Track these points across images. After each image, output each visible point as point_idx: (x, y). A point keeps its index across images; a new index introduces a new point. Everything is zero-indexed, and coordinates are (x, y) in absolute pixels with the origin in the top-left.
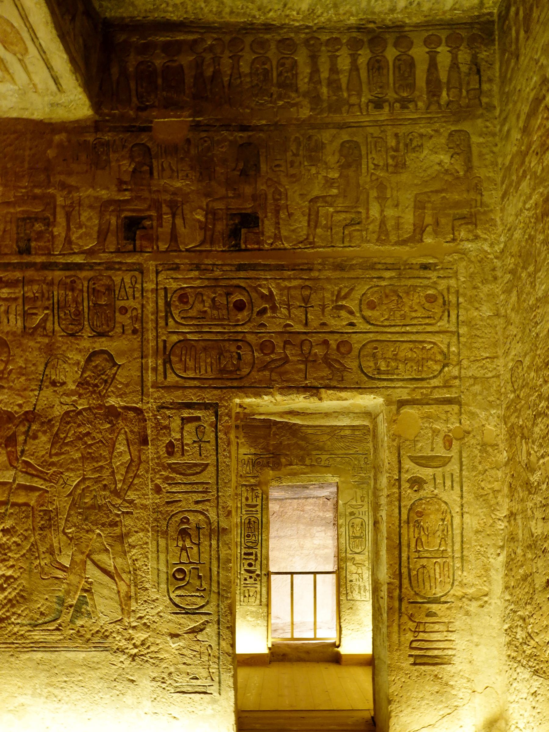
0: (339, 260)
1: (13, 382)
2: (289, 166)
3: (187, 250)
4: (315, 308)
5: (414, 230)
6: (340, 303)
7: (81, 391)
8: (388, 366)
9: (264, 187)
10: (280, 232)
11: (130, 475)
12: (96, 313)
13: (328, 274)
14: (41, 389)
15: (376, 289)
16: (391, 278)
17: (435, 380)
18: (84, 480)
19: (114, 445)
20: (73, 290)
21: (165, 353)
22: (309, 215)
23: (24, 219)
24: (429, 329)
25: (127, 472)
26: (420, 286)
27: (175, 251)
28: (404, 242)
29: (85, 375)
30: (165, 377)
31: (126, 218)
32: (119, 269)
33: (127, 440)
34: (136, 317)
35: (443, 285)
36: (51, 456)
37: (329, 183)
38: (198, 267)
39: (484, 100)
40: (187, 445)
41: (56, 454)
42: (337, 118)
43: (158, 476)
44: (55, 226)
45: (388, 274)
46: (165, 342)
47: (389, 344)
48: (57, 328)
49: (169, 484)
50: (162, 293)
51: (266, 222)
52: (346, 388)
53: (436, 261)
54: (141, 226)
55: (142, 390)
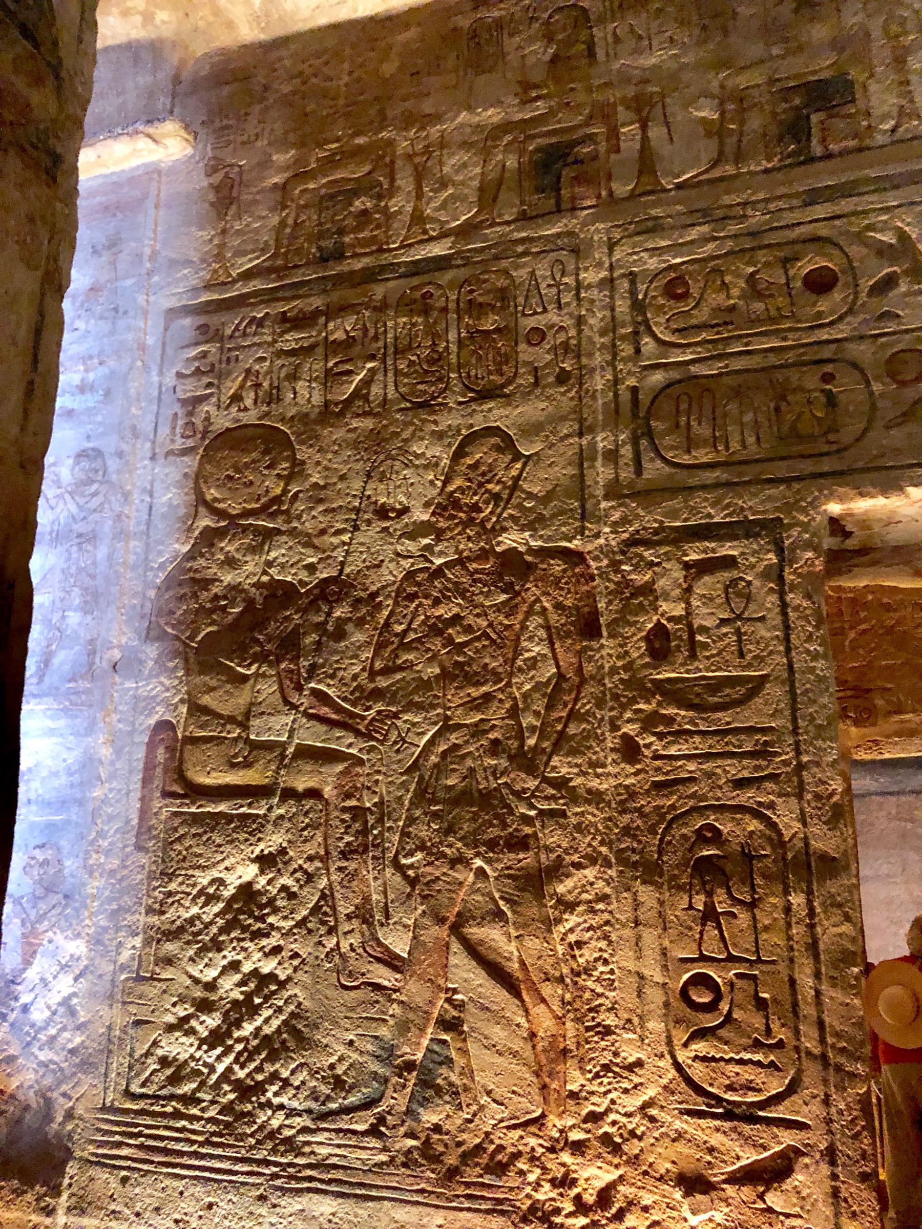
1: (299, 517)
3: (679, 187)
7: (442, 524)
10: (912, 101)
11: (555, 715)
12: (475, 352)
14: (356, 528)
18: (447, 728)
19: (518, 640)
20: (426, 311)
21: (635, 416)
23: (332, 197)
25: (549, 707)
29: (450, 488)
30: (639, 471)
31: (537, 150)
32: (525, 253)
33: (548, 628)
34: (566, 345)
36: (373, 674)
38: (705, 215)
40: (704, 630)
41: (386, 671)
43: (628, 715)
44: (391, 198)
46: (634, 390)
48: (391, 393)
49: (661, 736)
51: (873, 87)
54: (570, 159)
55: (583, 507)
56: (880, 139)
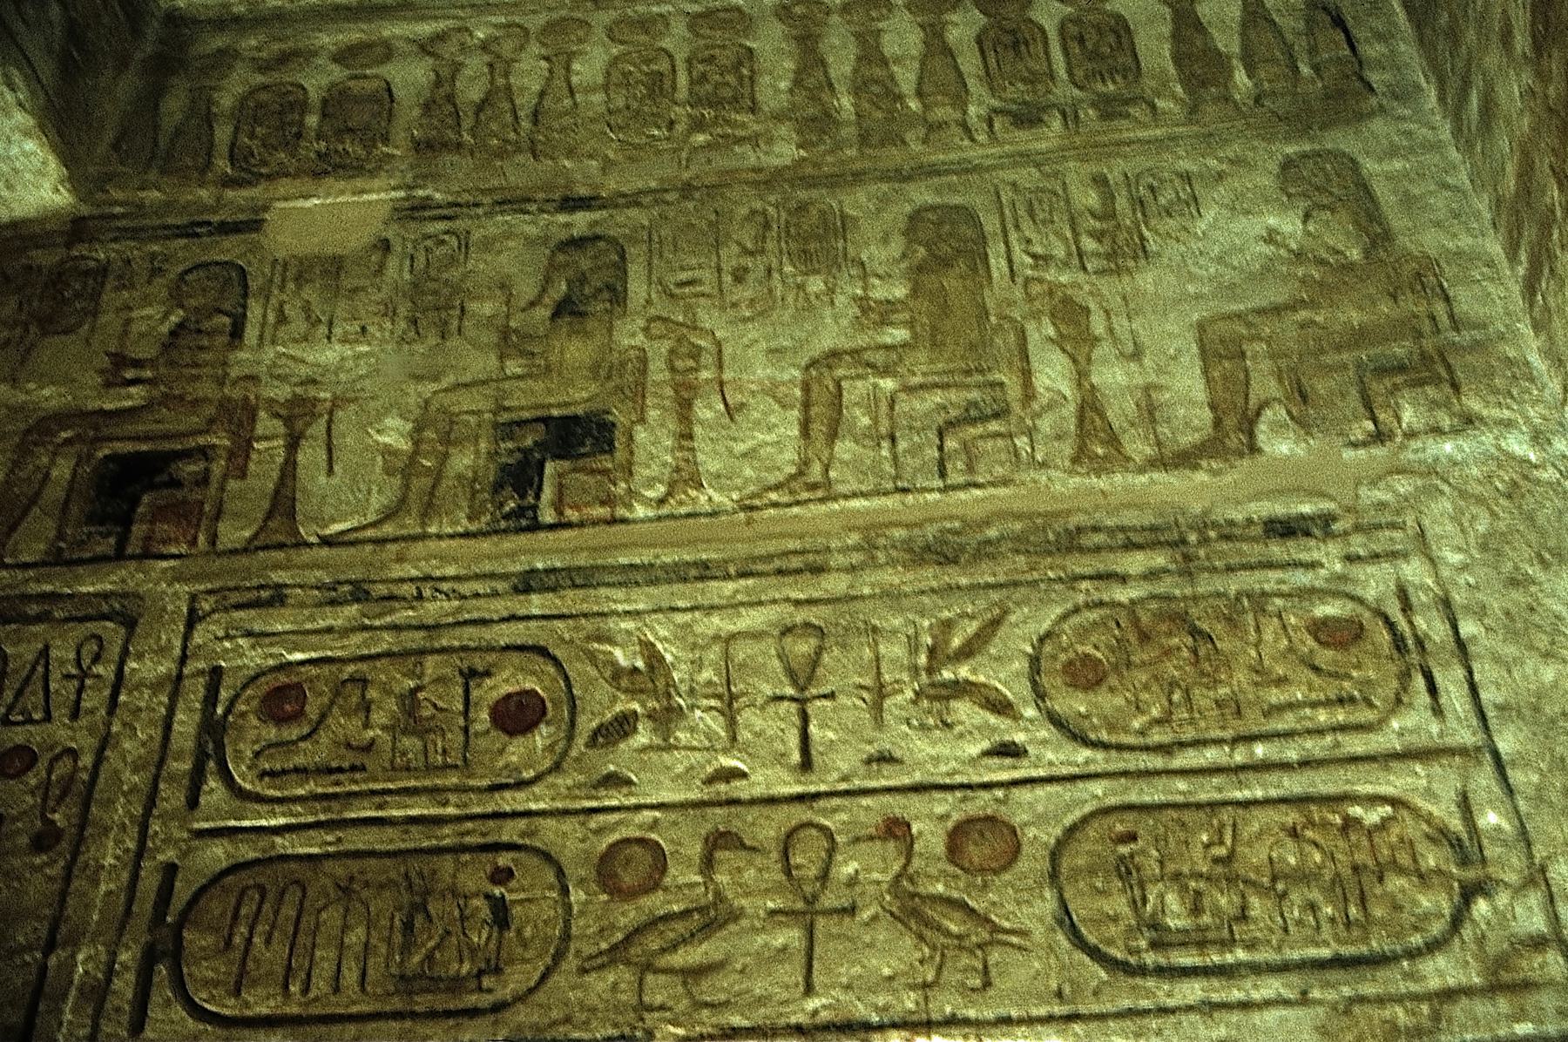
0: (931, 531)
2: (728, 279)
3: (327, 542)
4: (843, 700)
5: (1217, 423)
6: (947, 675)
8: (1196, 910)
9: (640, 339)
13: (890, 577)
15: (1093, 615)
16: (1152, 575)
17: (1441, 961)
22: (806, 405)
24: (1356, 744)
26: (1281, 595)
27: (281, 546)
28: (1185, 459)
32: (38, 619)
35: (1375, 583)
37: (885, 313)
39: (1374, 77)
42: (893, 156)
45: (1135, 563)
47: (1187, 816)
50: (195, 691)
51: (641, 435)
52: (1007, 1021)
53: (1327, 506)
56: (640, 511)
